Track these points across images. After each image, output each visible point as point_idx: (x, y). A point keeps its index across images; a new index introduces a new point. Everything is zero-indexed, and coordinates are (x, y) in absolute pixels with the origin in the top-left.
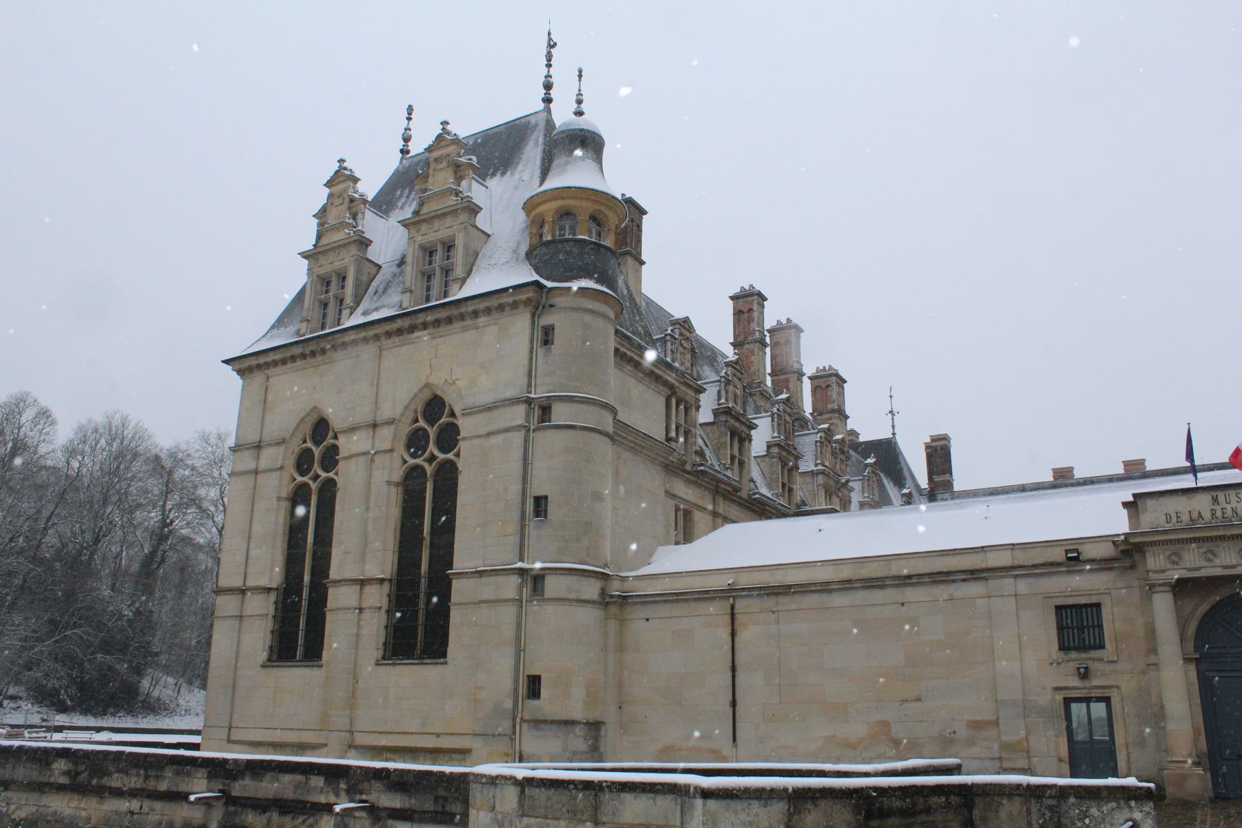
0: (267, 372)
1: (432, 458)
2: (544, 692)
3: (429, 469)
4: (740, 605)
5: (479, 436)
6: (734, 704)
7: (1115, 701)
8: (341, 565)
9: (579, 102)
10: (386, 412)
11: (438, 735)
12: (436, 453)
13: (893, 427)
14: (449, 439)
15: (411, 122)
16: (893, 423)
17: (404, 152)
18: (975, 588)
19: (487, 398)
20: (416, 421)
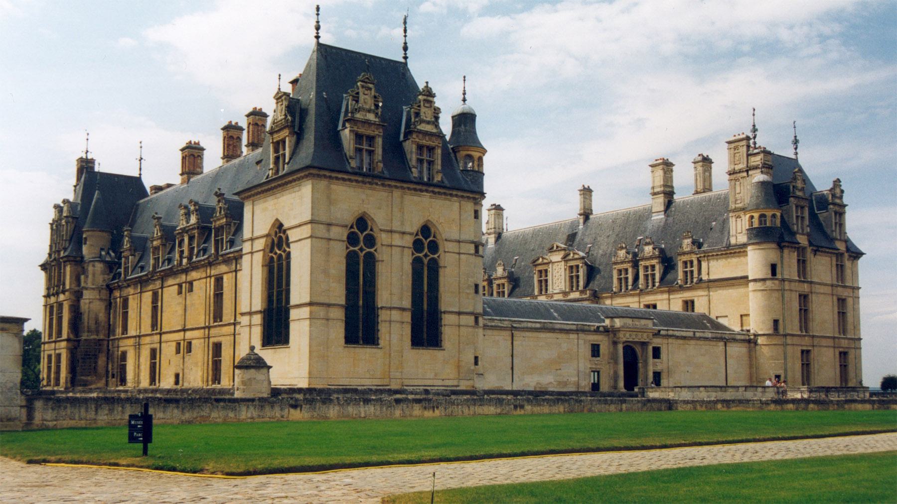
0: (331, 181)
1: (426, 256)
2: (480, 363)
3: (426, 261)
4: (515, 333)
5: (454, 253)
6: (512, 368)
7: (601, 373)
8: (383, 298)
9: (464, 94)
10: (408, 229)
12: (424, 253)
14: (434, 247)
15: (319, 16)
17: (317, 37)
18: (575, 336)
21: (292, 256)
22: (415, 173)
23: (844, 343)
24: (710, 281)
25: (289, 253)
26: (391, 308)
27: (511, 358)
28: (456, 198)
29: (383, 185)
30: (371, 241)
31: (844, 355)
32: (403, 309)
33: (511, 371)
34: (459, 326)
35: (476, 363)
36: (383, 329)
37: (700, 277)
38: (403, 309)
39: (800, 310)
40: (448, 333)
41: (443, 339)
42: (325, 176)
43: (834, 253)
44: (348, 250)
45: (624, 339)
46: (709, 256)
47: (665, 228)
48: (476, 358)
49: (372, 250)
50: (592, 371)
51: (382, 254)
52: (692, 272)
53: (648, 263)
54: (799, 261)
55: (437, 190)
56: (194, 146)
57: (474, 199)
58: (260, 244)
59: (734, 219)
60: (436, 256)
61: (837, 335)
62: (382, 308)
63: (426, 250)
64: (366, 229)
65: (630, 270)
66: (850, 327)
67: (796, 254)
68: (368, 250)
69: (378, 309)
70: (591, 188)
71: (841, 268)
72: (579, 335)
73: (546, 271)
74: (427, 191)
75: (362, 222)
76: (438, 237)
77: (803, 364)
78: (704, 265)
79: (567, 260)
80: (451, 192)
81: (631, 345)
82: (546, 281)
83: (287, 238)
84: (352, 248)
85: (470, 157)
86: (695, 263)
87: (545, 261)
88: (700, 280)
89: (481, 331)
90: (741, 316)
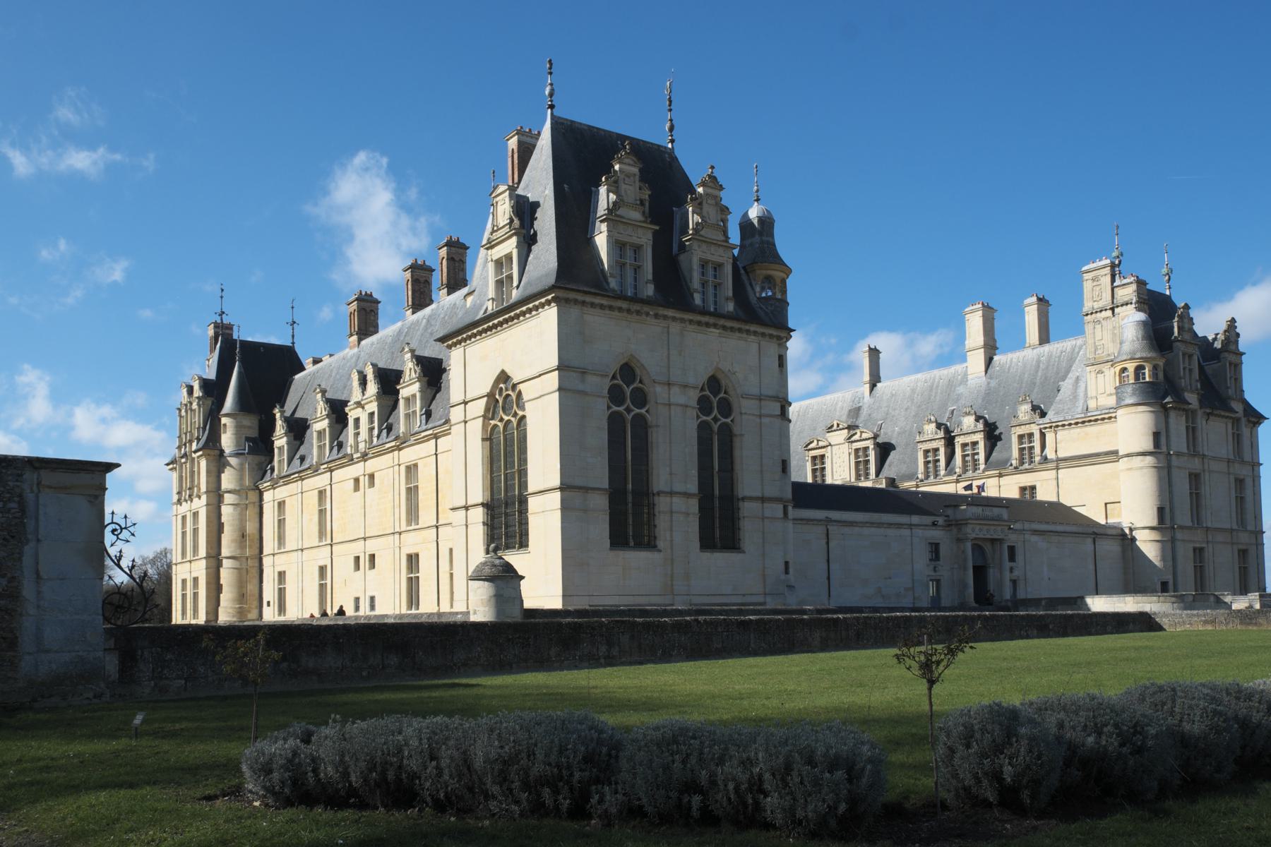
2: (791, 570)
3: (716, 427)
5: (754, 415)
6: (829, 578)
8: (660, 479)
10: (691, 380)
11: (744, 595)
12: (713, 416)
13: (293, 336)
14: (726, 408)
16: (293, 332)
19: (755, 391)
20: (725, 393)
21: (530, 422)
22: (698, 299)
23: (1244, 538)
24: (1059, 460)
25: (523, 417)
26: (672, 494)
27: (826, 564)
28: (753, 337)
29: (656, 316)
30: (641, 398)
31: (1243, 554)
32: (687, 495)
33: (827, 581)
34: (763, 518)
35: (787, 572)
36: (662, 522)
37: (1044, 454)
38: (687, 495)
39: (1191, 493)
40: (749, 532)
41: (741, 538)
42: (576, 302)
43: (1231, 418)
44: (610, 411)
45: (974, 536)
46: (1057, 426)
47: (989, 395)
48: (787, 563)
49: (643, 411)
50: (931, 580)
51: (656, 415)
52: (1031, 448)
53: (968, 439)
54: (1187, 428)
55: (729, 324)
56: (366, 298)
57: (779, 338)
58: (479, 407)
59: (1093, 375)
60: (728, 420)
61: (1235, 527)
62: (659, 493)
63: (715, 412)
64: (633, 381)
65: (942, 451)
66: (1249, 517)
67: (1184, 417)
68: (638, 411)
69: (654, 495)
70: (877, 348)
71: (1238, 438)
72: (913, 531)
73: (823, 457)
74: (715, 326)
75: (628, 371)
76: (731, 392)
77: (1195, 566)
78: (1050, 437)
79: (852, 442)
80: (747, 327)
81: (980, 543)
82: (823, 469)
83: (520, 394)
84: (615, 408)
85: (769, 281)
86: (1037, 437)
87: (821, 444)
88: (1045, 460)
89: (790, 525)
90: (1106, 504)
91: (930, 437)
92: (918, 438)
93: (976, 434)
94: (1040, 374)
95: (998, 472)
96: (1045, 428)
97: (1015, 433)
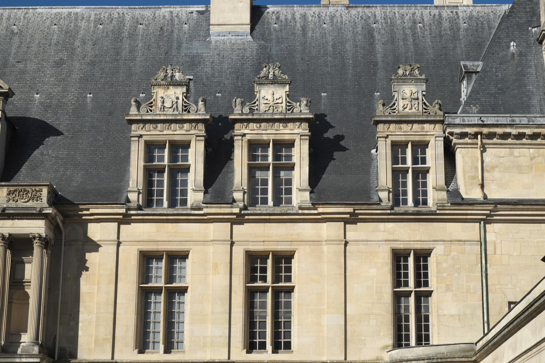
46: (491, 136)
91: (169, 114)
92: (133, 110)
93: (290, 125)
94: (379, 48)
95: (350, 210)
96: (463, 135)
97: (387, 137)
